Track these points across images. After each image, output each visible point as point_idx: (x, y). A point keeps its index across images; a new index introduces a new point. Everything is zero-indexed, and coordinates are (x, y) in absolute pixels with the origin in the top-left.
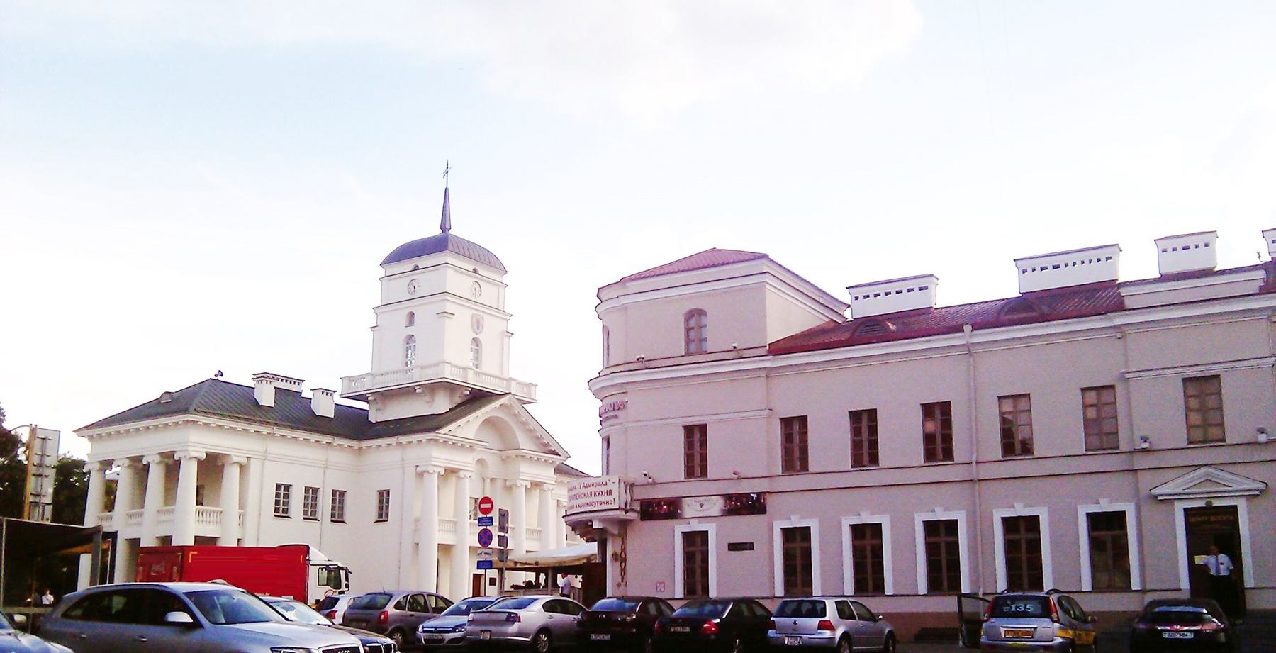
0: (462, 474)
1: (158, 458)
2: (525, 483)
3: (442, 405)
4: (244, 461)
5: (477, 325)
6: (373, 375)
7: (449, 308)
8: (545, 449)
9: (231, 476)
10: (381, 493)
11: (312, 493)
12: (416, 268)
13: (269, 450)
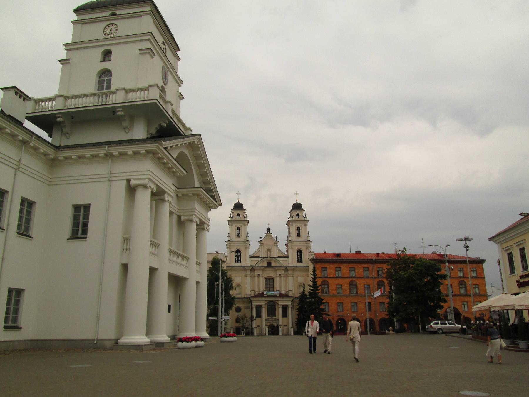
10: (77, 208)
12: (114, 14)
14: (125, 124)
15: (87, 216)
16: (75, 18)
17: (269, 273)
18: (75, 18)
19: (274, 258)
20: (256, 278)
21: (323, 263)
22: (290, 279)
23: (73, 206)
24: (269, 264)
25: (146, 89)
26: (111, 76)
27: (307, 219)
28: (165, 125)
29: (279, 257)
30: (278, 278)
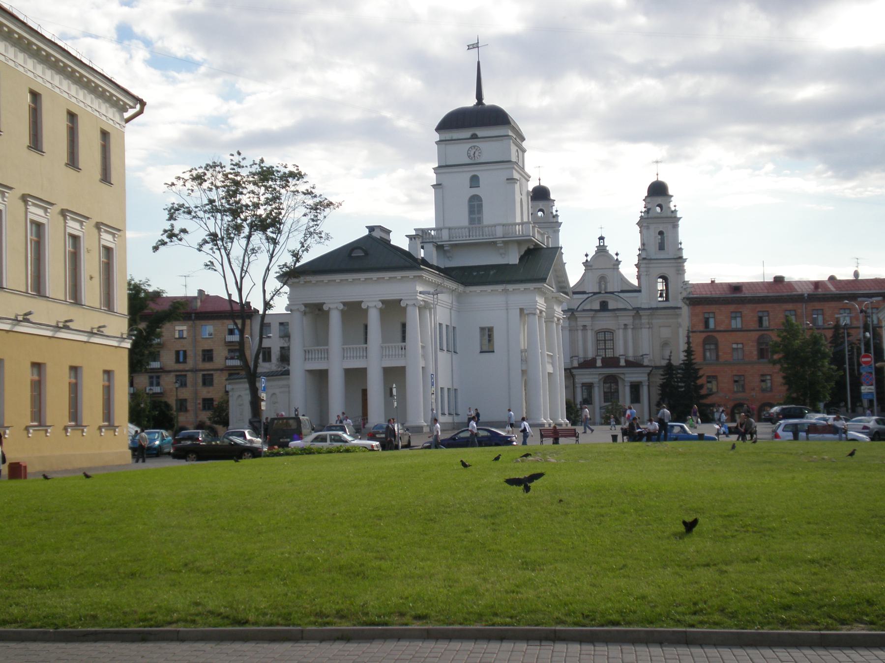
3: (513, 258)
12: (474, 137)
17: (605, 322)
18: (437, 137)
19: (612, 293)
20: (580, 332)
21: (708, 304)
22: (645, 333)
24: (604, 306)
27: (678, 216)
29: (622, 291)
30: (621, 331)
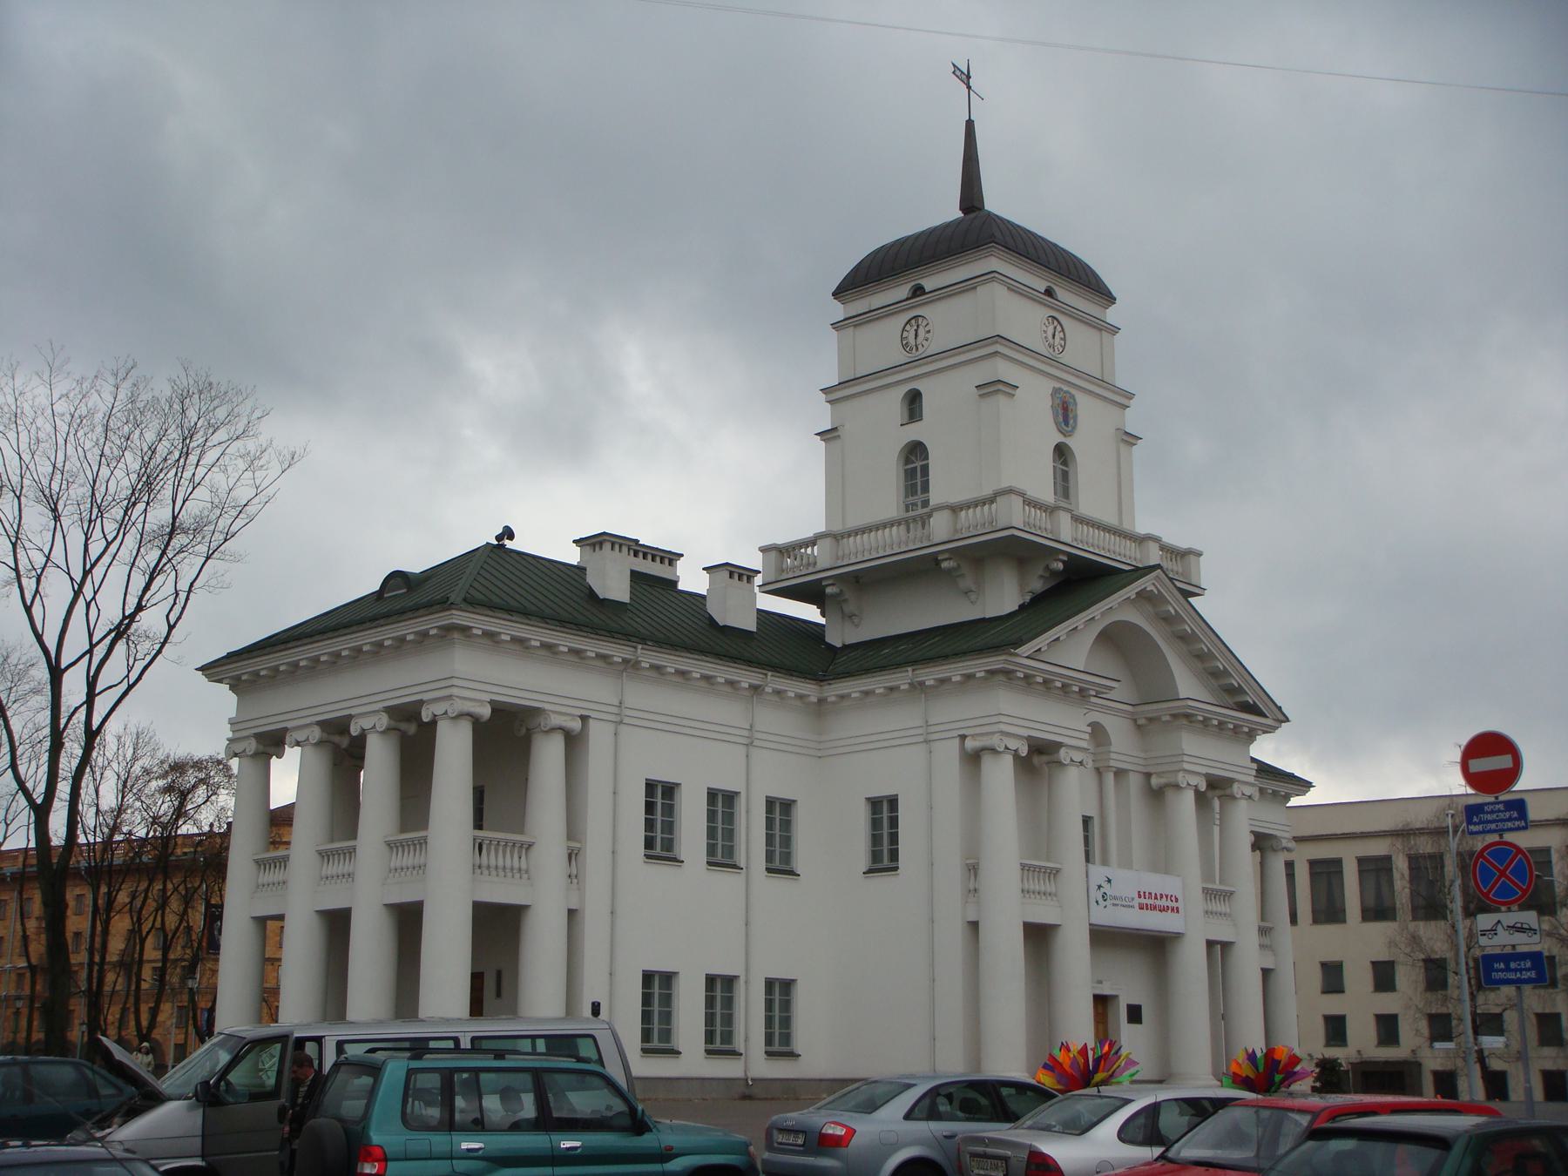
0: (1063, 754)
1: (383, 721)
2: (1194, 780)
4: (576, 725)
5: (1065, 414)
6: (835, 537)
7: (1004, 370)
8: (1230, 701)
9: (548, 757)
10: (875, 804)
11: (722, 803)
13: (630, 701)
14: (967, 582)
15: (894, 822)
16: (838, 311)
18: (838, 311)
23: (868, 799)
25: (991, 500)
26: (927, 458)
28: (1060, 566)
